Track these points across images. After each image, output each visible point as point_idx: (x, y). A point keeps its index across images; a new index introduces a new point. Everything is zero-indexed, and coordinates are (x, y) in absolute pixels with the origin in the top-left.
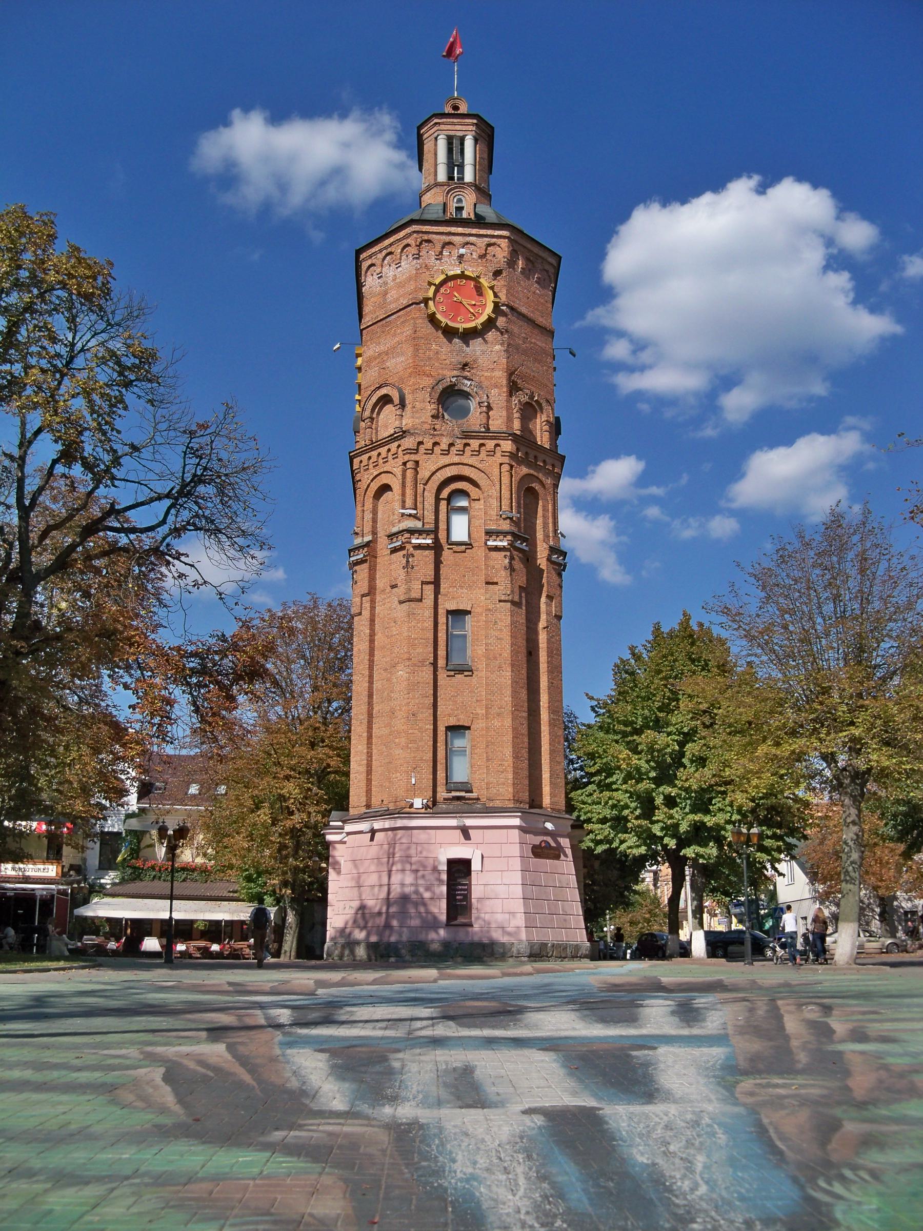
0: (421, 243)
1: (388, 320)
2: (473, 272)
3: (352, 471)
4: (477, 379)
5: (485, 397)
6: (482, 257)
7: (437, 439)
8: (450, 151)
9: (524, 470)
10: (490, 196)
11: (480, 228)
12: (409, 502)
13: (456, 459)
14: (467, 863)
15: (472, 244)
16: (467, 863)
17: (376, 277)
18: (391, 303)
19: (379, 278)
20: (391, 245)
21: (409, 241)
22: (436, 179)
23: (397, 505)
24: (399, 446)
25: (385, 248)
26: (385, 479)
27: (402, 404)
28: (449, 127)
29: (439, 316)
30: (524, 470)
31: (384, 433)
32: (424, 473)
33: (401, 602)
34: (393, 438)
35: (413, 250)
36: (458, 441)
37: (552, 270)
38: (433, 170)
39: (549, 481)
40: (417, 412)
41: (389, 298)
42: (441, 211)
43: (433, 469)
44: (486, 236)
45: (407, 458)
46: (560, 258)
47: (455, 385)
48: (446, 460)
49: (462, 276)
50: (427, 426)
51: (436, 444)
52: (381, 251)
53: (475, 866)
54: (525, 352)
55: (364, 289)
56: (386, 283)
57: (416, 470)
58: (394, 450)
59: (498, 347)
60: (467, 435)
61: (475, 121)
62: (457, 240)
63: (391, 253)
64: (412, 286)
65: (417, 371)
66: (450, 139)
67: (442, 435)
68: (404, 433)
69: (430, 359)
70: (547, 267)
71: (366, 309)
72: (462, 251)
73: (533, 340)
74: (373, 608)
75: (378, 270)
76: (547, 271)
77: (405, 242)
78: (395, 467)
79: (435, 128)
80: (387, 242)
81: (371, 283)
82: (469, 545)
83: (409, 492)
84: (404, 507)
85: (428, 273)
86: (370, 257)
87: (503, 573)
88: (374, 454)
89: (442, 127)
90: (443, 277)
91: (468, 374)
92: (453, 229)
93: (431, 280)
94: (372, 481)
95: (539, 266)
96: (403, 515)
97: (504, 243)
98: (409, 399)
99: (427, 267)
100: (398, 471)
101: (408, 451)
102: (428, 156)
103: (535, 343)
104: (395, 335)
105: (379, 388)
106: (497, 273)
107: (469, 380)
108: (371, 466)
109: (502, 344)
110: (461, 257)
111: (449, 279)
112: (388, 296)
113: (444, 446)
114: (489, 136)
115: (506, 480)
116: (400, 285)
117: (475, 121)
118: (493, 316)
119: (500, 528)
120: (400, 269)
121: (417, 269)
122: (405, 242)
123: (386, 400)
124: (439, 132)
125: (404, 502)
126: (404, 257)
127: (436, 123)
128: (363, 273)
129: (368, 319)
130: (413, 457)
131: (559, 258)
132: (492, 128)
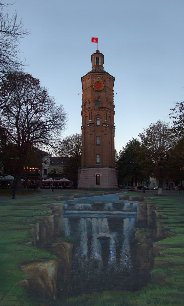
6: (102, 78)
8: (97, 60)
9: (109, 113)
13: (98, 112)
14: (100, 175)
16: (100, 175)
23: (88, 119)
27: (89, 103)
30: (109, 113)
32: (93, 114)
33: (89, 135)
34: (87, 109)
35: (90, 77)
39: (112, 115)
48: (96, 112)
49: (98, 82)
53: (101, 176)
57: (91, 114)
59: (104, 94)
60: (100, 108)
62: (98, 76)
65: (91, 98)
68: (90, 108)
72: (99, 77)
74: (85, 136)
78: (88, 113)
81: (84, 83)
82: (99, 125)
87: (105, 130)
95: (111, 79)
97: (105, 76)
98: (90, 102)
100: (89, 114)
105: (85, 101)
106: (104, 81)
109: (105, 93)
110: (98, 78)
111: (96, 82)
115: (106, 115)
123: (86, 103)
131: (114, 78)
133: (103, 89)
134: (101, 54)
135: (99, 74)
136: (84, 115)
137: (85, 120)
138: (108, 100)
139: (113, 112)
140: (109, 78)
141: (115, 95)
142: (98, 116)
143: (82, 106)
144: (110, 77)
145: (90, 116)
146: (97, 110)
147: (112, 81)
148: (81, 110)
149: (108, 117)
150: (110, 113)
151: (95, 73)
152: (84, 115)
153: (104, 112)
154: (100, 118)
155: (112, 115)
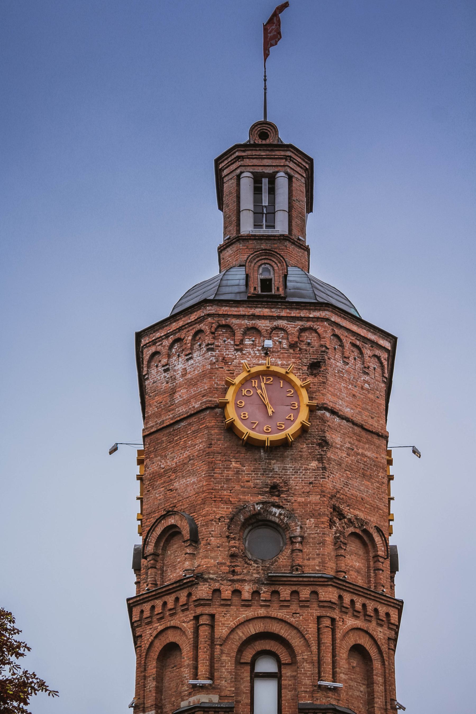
0: (216, 329)
1: (176, 427)
2: (282, 365)
3: (132, 624)
4: (288, 506)
5: (298, 530)
6: (292, 346)
7: (237, 586)
9: (351, 622)
10: (307, 249)
11: (291, 309)
12: (203, 669)
13: (262, 612)
15: (282, 329)
17: (161, 369)
18: (180, 405)
19: (165, 371)
20: (180, 329)
21: (202, 326)
22: (238, 231)
23: (186, 672)
24: (190, 595)
25: (173, 333)
26: (171, 637)
27: (194, 539)
28: (255, 162)
29: (240, 426)
30: (351, 622)
31: (173, 575)
32: (222, 631)
34: (181, 584)
36: (264, 589)
37: (384, 356)
38: (234, 218)
39: (381, 633)
40: (212, 550)
41: (178, 398)
42: (243, 282)
43: (232, 624)
44: (300, 319)
45: (199, 611)
46: (395, 339)
47: (259, 513)
50: (225, 569)
51: (237, 592)
52: (167, 336)
54: (349, 468)
55: (147, 382)
56: (173, 379)
57: (212, 627)
58: (183, 599)
59: (314, 464)
60: (273, 580)
61: (289, 153)
62: (263, 325)
63: (178, 340)
64: (205, 386)
66: (257, 179)
67: (243, 581)
69: (228, 480)
70: (378, 352)
71: (150, 411)
72: (268, 343)
73: (360, 451)
75: (164, 361)
76: (379, 358)
77: (198, 327)
79: (238, 164)
80: (175, 326)
81: (156, 375)
83: (203, 656)
84: (195, 677)
85: (226, 368)
86: (154, 343)
88: (159, 603)
89: (247, 162)
90: (244, 375)
91: (276, 499)
92: (258, 311)
93: (228, 379)
94: (156, 637)
95: (367, 352)
96: (194, 686)
98: (203, 531)
99: (224, 360)
100: (188, 627)
101: (200, 602)
102: (229, 199)
103: (363, 455)
104: (185, 448)
105: (163, 517)
107: (278, 507)
108: (155, 619)
109: (320, 460)
112: (177, 395)
113: (246, 596)
114: (306, 170)
115: (327, 639)
116: (192, 383)
117: (289, 153)
118: (308, 424)
119: (318, 702)
120: (191, 362)
121: (212, 364)
122: (198, 327)
123: (172, 533)
124: (242, 169)
125: (196, 668)
126: (196, 346)
127: (238, 157)
128: (145, 363)
129: (151, 424)
130: (207, 610)
131: (393, 340)
132: (311, 161)
133: (304, 430)
134: (290, 147)
135: (275, 312)
136: (148, 633)
137: (159, 678)
138: (341, 516)
139: (382, 610)
140: (347, 340)
141: (402, 467)
142: (266, 642)
143: (139, 554)
144: (363, 332)
145: (196, 647)
146: (256, 593)
147: (373, 364)
148: (133, 593)
149: (343, 654)
150: (358, 623)
151: (242, 310)
152: (148, 633)
153: (315, 612)
154: (285, 658)
155: (381, 633)
